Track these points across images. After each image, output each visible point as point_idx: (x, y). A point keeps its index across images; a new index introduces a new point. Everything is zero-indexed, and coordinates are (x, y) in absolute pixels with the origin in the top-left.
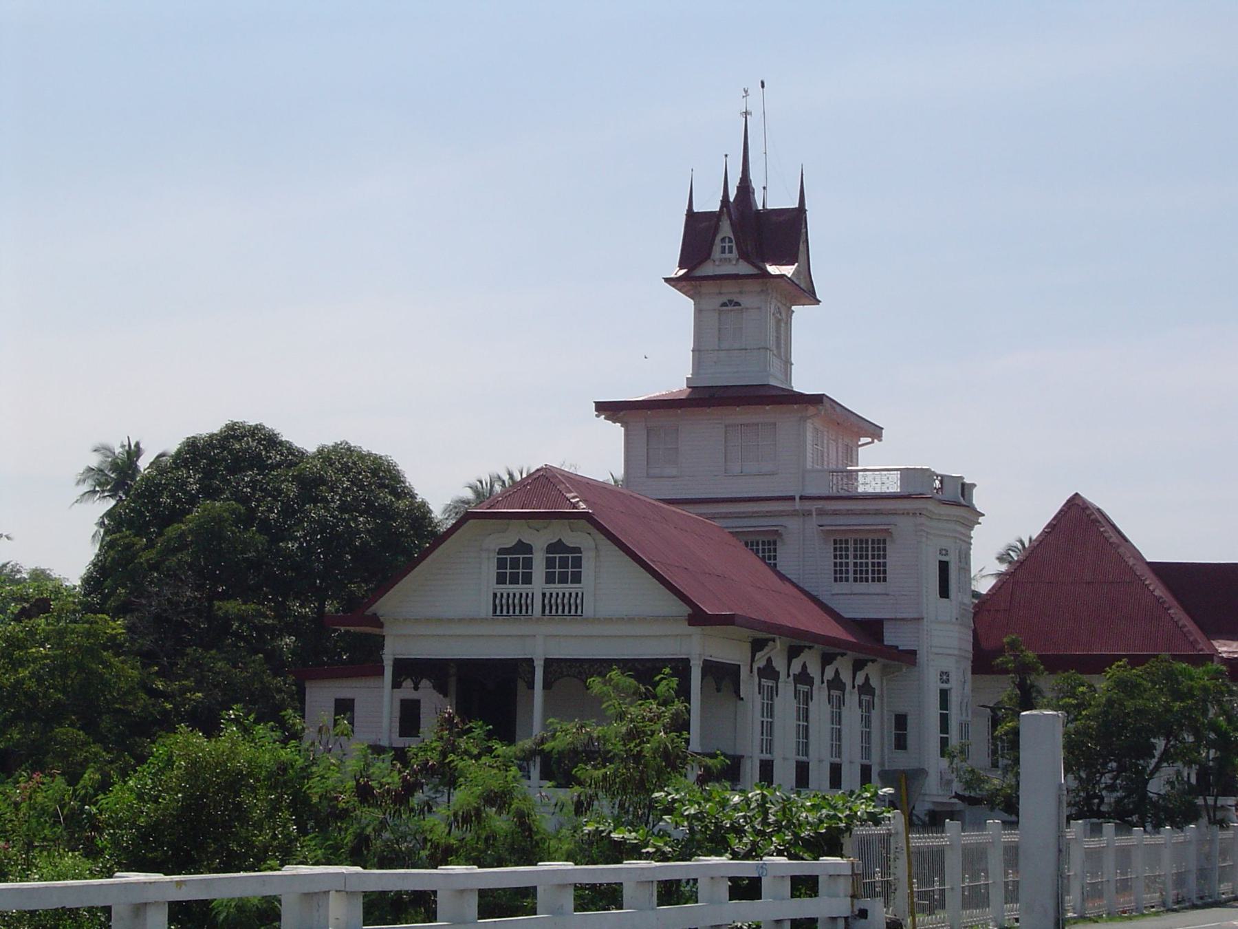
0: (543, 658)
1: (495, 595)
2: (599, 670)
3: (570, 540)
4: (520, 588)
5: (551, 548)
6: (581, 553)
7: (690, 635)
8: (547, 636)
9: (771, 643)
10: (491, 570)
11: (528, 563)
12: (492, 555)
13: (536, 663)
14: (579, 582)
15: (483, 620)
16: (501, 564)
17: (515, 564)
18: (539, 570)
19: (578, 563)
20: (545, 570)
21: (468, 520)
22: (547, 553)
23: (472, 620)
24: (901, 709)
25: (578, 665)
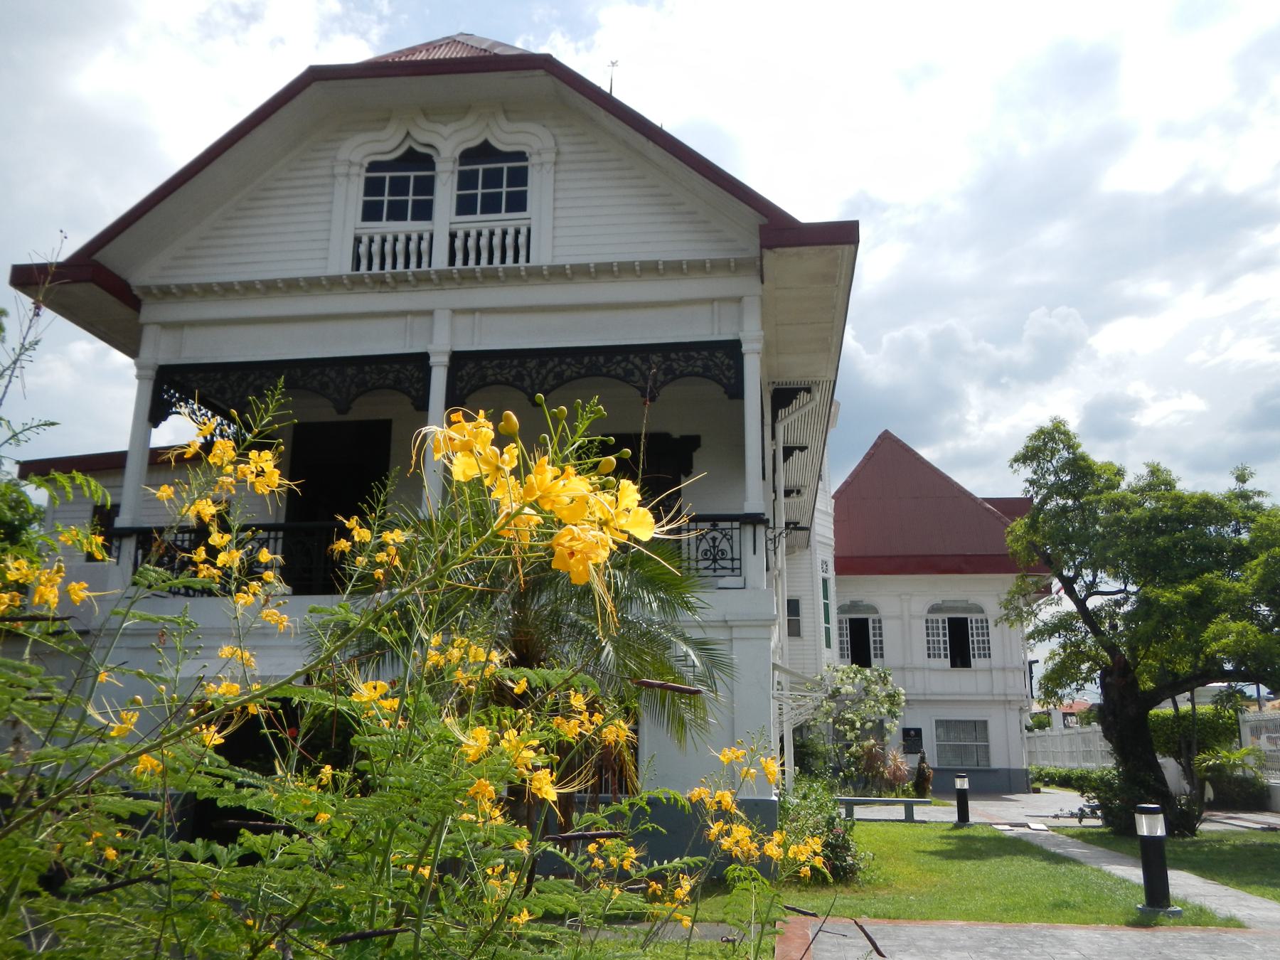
0: (448, 348)
1: (358, 241)
2: (558, 369)
3: (505, 137)
4: (410, 226)
5: (468, 156)
6: (526, 160)
7: (739, 300)
8: (455, 312)
9: (803, 396)
10: (352, 195)
11: (426, 186)
12: (355, 170)
13: (433, 360)
15: (334, 283)
16: (373, 187)
17: (399, 186)
18: (445, 194)
19: (519, 177)
20: (455, 192)
22: (461, 164)
23: (313, 285)
24: (794, 596)
25: (515, 362)
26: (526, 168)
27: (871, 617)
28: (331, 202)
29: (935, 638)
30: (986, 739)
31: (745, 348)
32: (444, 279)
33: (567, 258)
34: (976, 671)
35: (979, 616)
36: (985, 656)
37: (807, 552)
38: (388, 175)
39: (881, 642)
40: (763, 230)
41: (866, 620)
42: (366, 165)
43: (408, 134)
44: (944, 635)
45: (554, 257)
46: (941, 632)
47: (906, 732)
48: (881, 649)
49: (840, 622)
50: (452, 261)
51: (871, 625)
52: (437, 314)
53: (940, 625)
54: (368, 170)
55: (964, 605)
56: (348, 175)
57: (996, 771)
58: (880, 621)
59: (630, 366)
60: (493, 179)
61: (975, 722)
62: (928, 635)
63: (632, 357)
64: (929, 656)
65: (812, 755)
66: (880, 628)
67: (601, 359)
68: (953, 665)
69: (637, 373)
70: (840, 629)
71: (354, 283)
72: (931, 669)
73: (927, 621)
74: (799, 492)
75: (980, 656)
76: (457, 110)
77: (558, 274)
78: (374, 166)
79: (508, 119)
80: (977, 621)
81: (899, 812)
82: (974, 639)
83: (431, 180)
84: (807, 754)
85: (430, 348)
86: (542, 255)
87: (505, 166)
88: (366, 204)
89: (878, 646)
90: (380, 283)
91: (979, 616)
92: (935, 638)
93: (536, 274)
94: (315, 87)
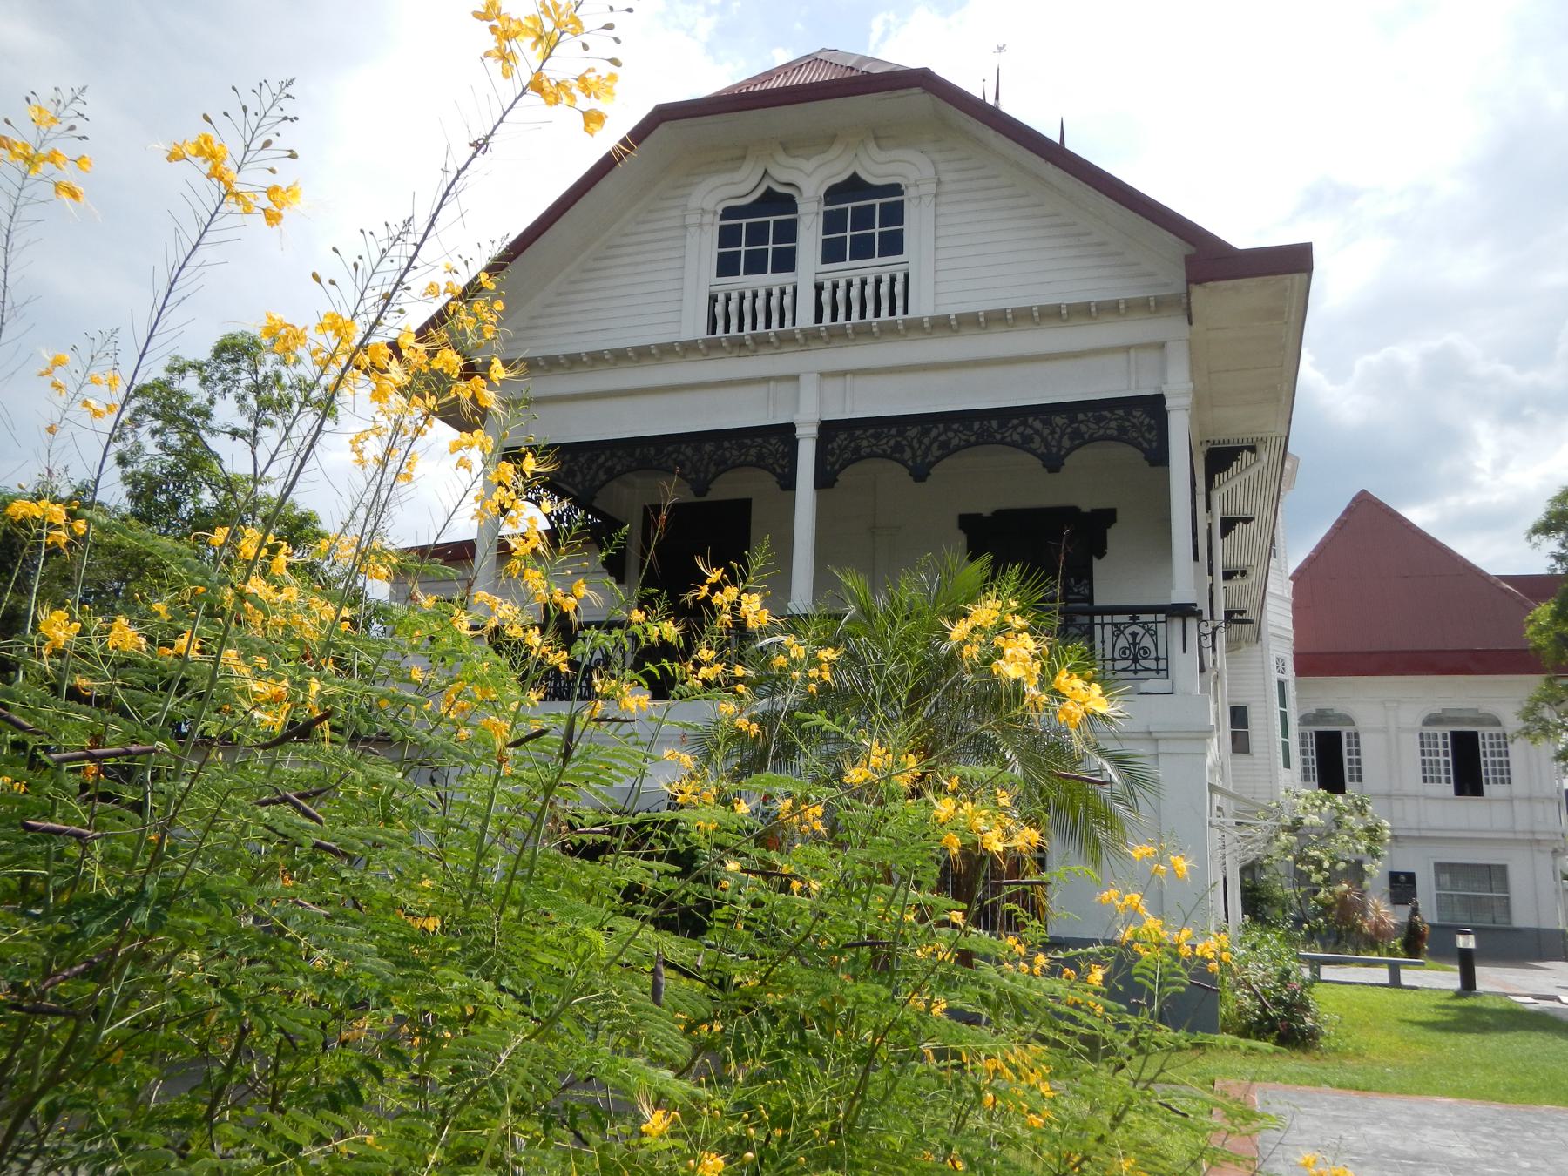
0: (816, 418)
1: (713, 299)
2: (943, 438)
4: (771, 280)
5: (834, 194)
6: (902, 193)
7: (1162, 346)
8: (823, 375)
9: (1246, 457)
10: (707, 247)
11: (788, 231)
12: (708, 218)
13: (799, 432)
14: (899, 251)
15: (689, 348)
16: (728, 236)
17: (758, 234)
19: (894, 214)
20: (821, 237)
21: (663, 120)
22: (826, 205)
24: (1240, 702)
25: (894, 431)
26: (902, 202)
27: (1345, 730)
28: (683, 257)
29: (1433, 758)
30: (1505, 888)
31: (1169, 404)
32: (810, 338)
33: (952, 307)
34: (1490, 800)
35: (1495, 730)
36: (1503, 781)
37: (1258, 647)
38: (744, 222)
39: (1359, 762)
40: (1189, 261)
41: (1337, 735)
42: (720, 212)
43: (766, 172)
44: (1446, 754)
45: (936, 305)
46: (1441, 749)
47: (1394, 877)
48: (1359, 770)
49: (1303, 735)
50: (819, 317)
51: (1344, 740)
52: (802, 379)
53: (1440, 741)
54: (722, 218)
55: (1472, 715)
56: (700, 225)
57: (1519, 931)
58: (1357, 735)
59: (1029, 431)
60: (863, 218)
61: (1489, 866)
62: (1423, 753)
63: (1030, 420)
64: (1425, 780)
65: (1267, 900)
66: (1357, 744)
67: (994, 424)
68: (1460, 791)
69: (1037, 439)
70: (1303, 744)
71: (711, 348)
72: (1427, 797)
73: (1421, 736)
74: (1244, 573)
75: (1495, 781)
76: (825, 140)
77: (942, 325)
78: (729, 213)
79: (879, 147)
80: (1491, 736)
81: (1382, 975)
82: (1487, 760)
83: (792, 225)
84: (1261, 900)
85: (796, 419)
86: (922, 306)
87: (877, 202)
88: (721, 257)
89: (1355, 766)
90: (739, 345)
91: (1495, 730)
92: (1433, 758)
93: (916, 327)
94: (663, 128)
